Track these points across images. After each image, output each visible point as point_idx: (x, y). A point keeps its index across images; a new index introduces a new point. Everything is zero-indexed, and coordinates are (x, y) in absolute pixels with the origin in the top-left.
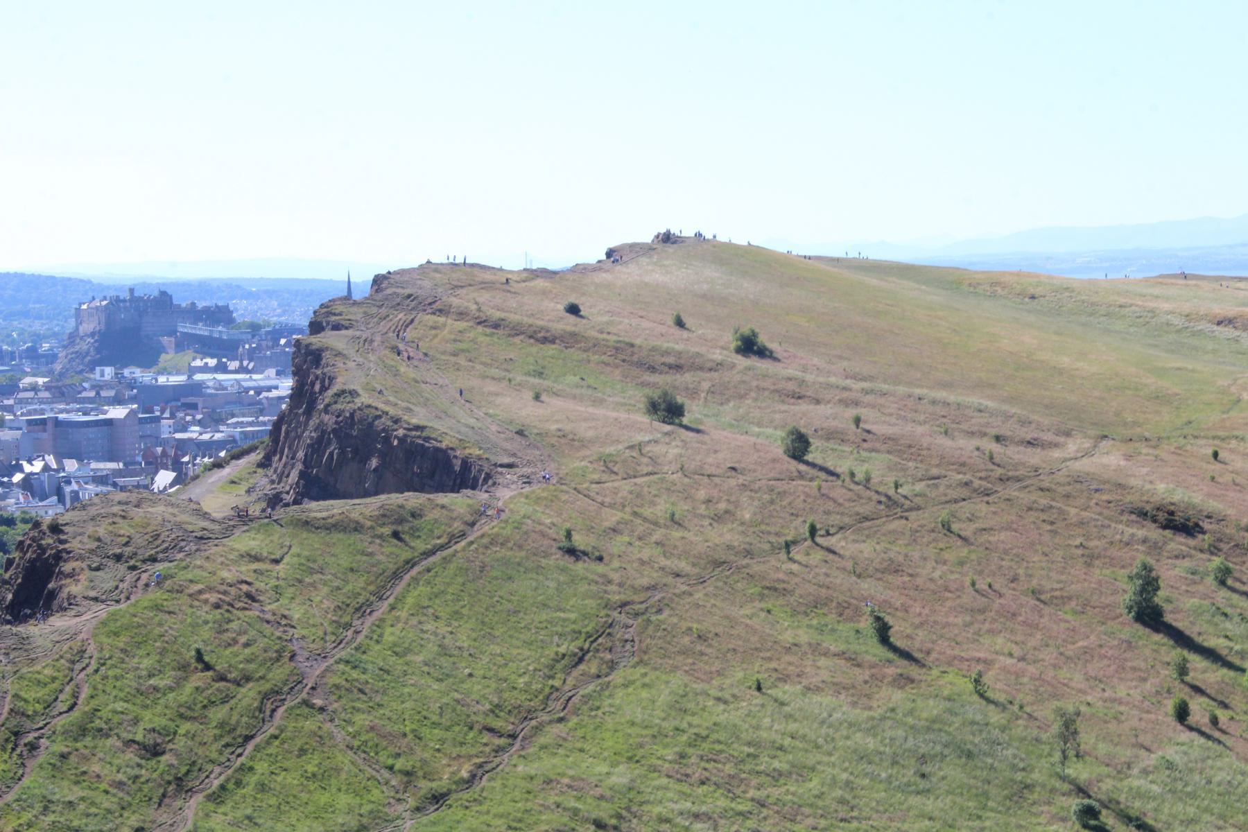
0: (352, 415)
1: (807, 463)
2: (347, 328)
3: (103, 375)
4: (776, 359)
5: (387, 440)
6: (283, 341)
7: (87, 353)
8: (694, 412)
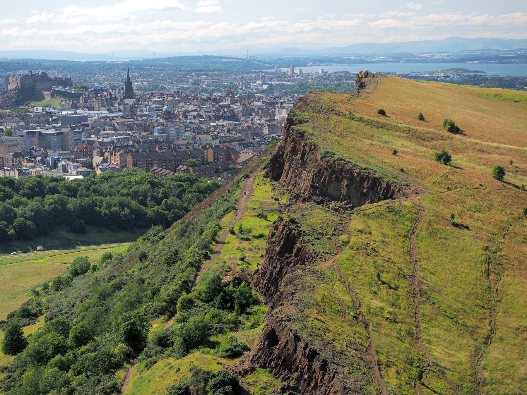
0: (334, 163)
1: (502, 181)
2: (306, 122)
3: (37, 110)
4: (465, 135)
5: (351, 174)
6: (99, 95)
7: (13, 98)
8: (455, 158)
